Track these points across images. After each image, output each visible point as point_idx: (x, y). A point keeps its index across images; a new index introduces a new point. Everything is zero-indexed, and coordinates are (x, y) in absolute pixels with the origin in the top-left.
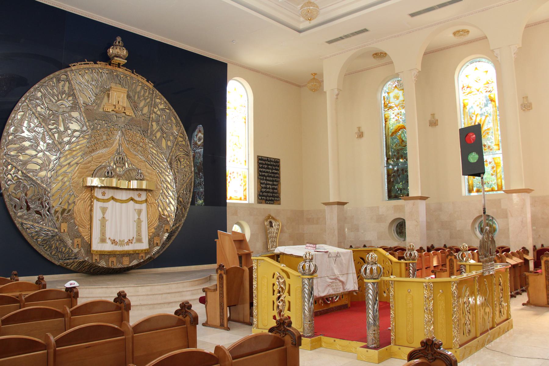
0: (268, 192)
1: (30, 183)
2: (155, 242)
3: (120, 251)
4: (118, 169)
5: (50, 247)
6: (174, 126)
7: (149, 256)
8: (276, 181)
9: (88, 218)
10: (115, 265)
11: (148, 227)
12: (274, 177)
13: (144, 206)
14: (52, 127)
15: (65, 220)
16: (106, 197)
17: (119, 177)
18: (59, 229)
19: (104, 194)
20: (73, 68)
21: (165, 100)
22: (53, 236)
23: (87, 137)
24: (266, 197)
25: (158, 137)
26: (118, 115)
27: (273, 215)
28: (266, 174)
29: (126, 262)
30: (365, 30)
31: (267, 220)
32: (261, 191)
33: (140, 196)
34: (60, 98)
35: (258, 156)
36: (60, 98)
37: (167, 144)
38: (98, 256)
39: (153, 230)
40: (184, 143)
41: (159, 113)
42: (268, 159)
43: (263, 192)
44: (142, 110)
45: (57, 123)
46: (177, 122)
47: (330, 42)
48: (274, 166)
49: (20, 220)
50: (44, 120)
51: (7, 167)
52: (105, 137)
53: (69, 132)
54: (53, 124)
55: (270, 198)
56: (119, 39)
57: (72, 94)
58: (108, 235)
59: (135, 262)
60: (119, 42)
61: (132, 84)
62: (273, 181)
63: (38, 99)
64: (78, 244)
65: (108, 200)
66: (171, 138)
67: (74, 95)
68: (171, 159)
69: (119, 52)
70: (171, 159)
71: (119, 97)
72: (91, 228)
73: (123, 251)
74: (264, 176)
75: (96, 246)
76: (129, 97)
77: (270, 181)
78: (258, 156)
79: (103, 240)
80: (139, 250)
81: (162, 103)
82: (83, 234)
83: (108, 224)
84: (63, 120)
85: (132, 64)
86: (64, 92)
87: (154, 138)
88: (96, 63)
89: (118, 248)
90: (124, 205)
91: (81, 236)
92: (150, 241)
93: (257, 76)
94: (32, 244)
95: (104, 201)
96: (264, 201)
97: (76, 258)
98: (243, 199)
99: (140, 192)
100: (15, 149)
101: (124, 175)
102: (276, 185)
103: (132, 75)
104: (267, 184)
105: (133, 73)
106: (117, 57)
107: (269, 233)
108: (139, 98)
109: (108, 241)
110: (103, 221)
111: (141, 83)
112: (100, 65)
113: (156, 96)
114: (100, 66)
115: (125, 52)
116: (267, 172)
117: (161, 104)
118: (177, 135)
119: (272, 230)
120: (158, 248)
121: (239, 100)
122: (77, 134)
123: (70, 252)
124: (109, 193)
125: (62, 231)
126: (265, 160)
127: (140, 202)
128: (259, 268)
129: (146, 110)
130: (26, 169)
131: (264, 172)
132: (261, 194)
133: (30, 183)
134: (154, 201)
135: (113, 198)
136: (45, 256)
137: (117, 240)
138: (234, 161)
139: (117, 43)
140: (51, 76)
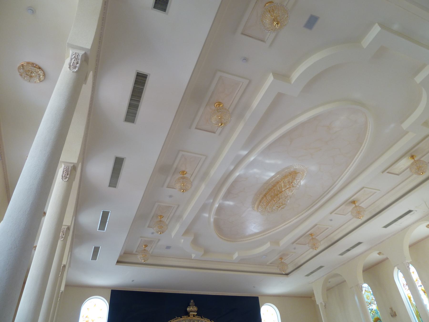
30: (321, 267)
47: (308, 275)
56: (192, 301)
69: (192, 309)
85: (200, 314)
88: (181, 318)
105: (202, 318)
106: (191, 312)
112: (185, 318)
115: (195, 309)
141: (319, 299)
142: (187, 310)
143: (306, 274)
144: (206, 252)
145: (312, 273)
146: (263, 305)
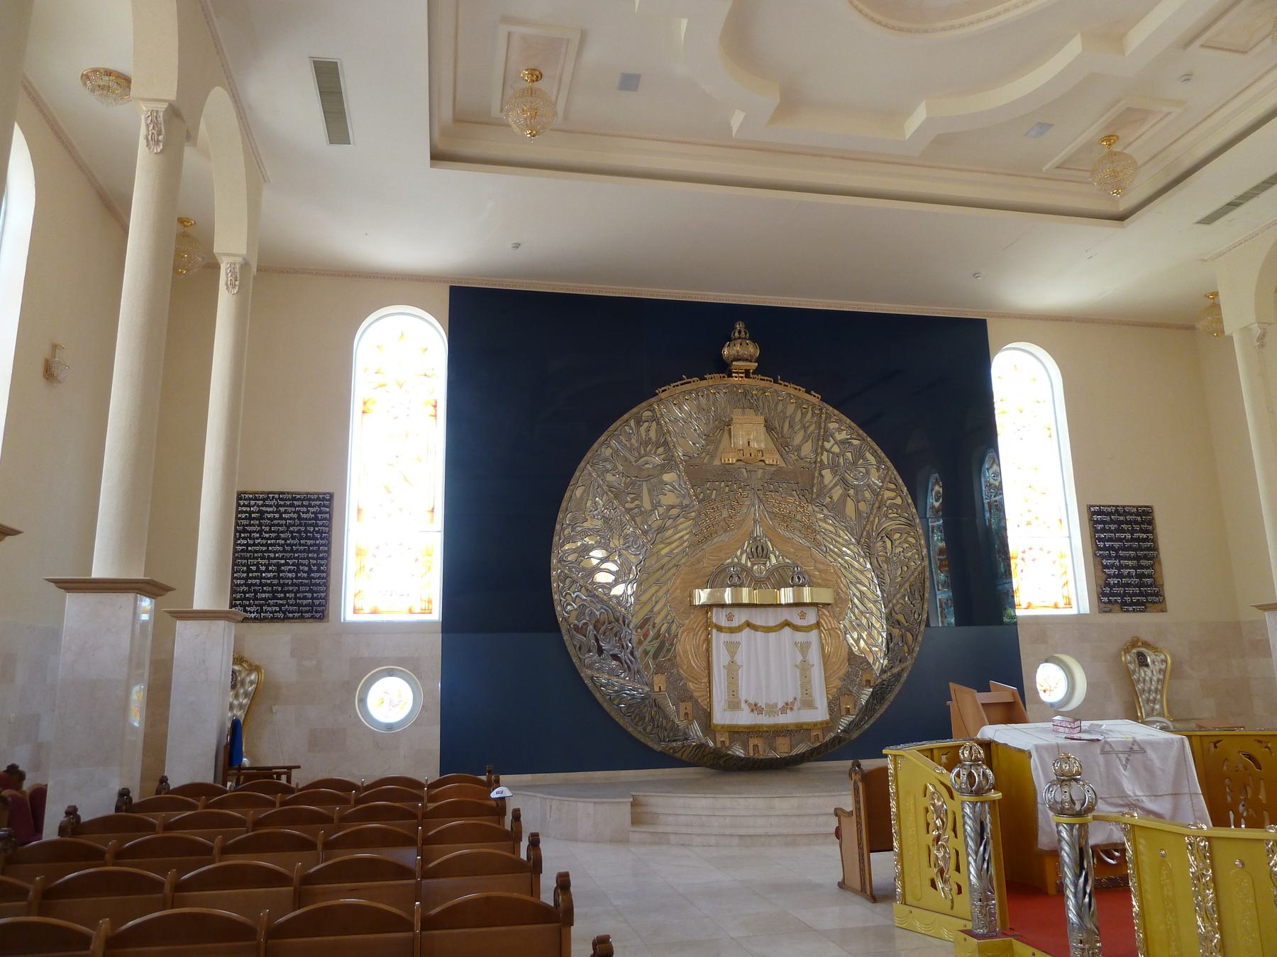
0: (1128, 585)
2: (843, 706)
3: (768, 726)
6: (873, 471)
8: (1145, 557)
9: (704, 664)
11: (826, 678)
12: (1140, 549)
13: (814, 633)
15: (659, 669)
16: (736, 623)
17: (757, 583)
18: (651, 686)
19: (730, 618)
20: (663, 395)
21: (848, 421)
22: (643, 699)
25: (836, 498)
28: (1117, 545)
29: (783, 749)
31: (1127, 651)
32: (1107, 585)
33: (803, 616)
37: (858, 511)
39: (838, 683)
40: (899, 501)
41: (836, 449)
42: (1118, 511)
43: (1111, 587)
44: (799, 449)
45: (638, 497)
46: (880, 461)
47: (1209, 220)
49: (589, 672)
50: (617, 494)
51: (564, 582)
52: (725, 514)
53: (661, 510)
54: (633, 500)
56: (739, 326)
57: (664, 444)
58: (743, 695)
59: (801, 749)
60: (740, 332)
61: (777, 404)
62: (1138, 558)
63: (605, 460)
66: (867, 495)
67: (666, 443)
68: (869, 536)
69: (741, 350)
70: (869, 536)
71: (749, 435)
72: (710, 682)
73: (774, 726)
75: (721, 717)
76: (769, 428)
77: (1129, 558)
79: (734, 705)
80: (808, 724)
81: (841, 430)
82: (696, 694)
83: (742, 675)
85: (768, 367)
87: (828, 500)
91: (691, 697)
92: (833, 705)
93: (1057, 330)
94: (613, 714)
95: (732, 630)
96: (1117, 607)
98: (1061, 605)
99: (805, 609)
100: (574, 551)
102: (1148, 568)
104: (1121, 567)
105: (776, 382)
108: (791, 426)
109: (743, 705)
111: (791, 399)
112: (713, 380)
113: (829, 417)
115: (752, 349)
116: (1119, 540)
117: (840, 430)
118: (881, 488)
119: (1146, 673)
121: (1026, 393)
122: (674, 512)
123: (675, 728)
124: (740, 617)
125: (657, 689)
127: (808, 629)
129: (807, 449)
130: (593, 583)
131: (1110, 540)
132: (1107, 590)
134: (834, 623)
135: (748, 624)
136: (635, 734)
137: (762, 704)
138: (1029, 523)
140: (626, 416)
141: (1238, 316)
143: (1198, 218)
144: (791, 102)
145: (1233, 205)
146: (998, 350)
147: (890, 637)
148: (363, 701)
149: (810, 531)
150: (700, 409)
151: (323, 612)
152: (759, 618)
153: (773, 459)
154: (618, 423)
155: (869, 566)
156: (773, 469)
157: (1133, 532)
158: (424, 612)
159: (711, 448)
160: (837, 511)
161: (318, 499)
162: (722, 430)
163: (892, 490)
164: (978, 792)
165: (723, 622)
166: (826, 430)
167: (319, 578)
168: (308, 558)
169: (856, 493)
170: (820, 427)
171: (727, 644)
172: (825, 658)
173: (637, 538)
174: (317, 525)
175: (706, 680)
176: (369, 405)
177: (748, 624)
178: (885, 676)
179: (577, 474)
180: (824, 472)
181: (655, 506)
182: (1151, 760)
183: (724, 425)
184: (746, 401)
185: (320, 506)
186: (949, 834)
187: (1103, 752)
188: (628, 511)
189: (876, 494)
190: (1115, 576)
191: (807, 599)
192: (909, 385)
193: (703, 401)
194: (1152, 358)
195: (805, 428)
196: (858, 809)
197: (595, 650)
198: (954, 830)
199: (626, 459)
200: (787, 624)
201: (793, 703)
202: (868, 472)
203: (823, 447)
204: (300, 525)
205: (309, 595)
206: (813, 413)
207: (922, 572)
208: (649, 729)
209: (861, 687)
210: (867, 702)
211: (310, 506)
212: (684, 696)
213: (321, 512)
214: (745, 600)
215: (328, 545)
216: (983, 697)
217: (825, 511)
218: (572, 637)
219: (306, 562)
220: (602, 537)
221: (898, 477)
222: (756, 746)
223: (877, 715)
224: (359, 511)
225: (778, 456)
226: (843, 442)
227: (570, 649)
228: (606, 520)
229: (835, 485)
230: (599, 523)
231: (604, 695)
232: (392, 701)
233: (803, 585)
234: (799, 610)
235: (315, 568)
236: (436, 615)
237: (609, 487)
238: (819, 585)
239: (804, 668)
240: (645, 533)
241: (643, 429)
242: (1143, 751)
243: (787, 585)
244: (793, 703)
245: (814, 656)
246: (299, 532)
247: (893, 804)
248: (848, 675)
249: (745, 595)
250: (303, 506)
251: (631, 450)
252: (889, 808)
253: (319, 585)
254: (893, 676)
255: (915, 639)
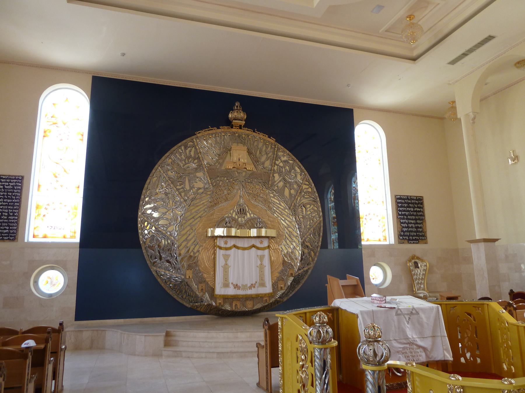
0: (412, 231)
1: (161, 236)
2: (279, 286)
3: (243, 295)
4: (240, 219)
5: (181, 291)
7: (273, 299)
8: (419, 219)
9: (212, 265)
10: (238, 307)
11: (272, 272)
12: (417, 215)
13: (267, 251)
14: (180, 187)
15: (190, 267)
16: (228, 245)
17: (240, 226)
18: (185, 276)
19: (226, 243)
20: (199, 135)
21: (288, 152)
22: (181, 282)
23: (209, 193)
24: (409, 236)
26: (239, 171)
27: (418, 254)
28: (407, 213)
29: (249, 306)
31: (410, 261)
32: (402, 231)
33: (261, 242)
34: (187, 162)
35: (396, 196)
36: (187, 162)
38: (222, 300)
39: (277, 275)
40: (310, 190)
41: (281, 164)
42: (409, 198)
43: (404, 232)
45: (183, 183)
46: (302, 171)
47: (453, 62)
48: (416, 203)
49: (155, 268)
53: (194, 190)
55: (414, 238)
56: (237, 104)
57: (198, 158)
58: (231, 280)
59: (258, 306)
60: (237, 107)
61: (254, 142)
62: (416, 219)
63: (168, 165)
64: (202, 289)
65: (230, 248)
66: (295, 186)
67: (198, 158)
68: (295, 205)
69: (237, 115)
70: (295, 205)
71: (239, 155)
72: (214, 274)
73: (246, 295)
74: (405, 215)
75: (219, 290)
76: (249, 153)
77: (412, 220)
78: (396, 196)
80: (262, 294)
81: (285, 156)
82: (207, 280)
83: (231, 270)
84: (189, 181)
86: (190, 157)
87: (276, 188)
88: (218, 128)
89: (240, 292)
90: (246, 252)
91: (205, 281)
92: (275, 286)
93: (384, 115)
94: (166, 289)
95: (226, 249)
96: (406, 241)
97: (202, 302)
98: (382, 240)
99: (262, 239)
100: (150, 208)
101: (245, 224)
102: (420, 224)
103: (254, 134)
104: (409, 223)
105: (254, 132)
106: (236, 120)
107: (414, 274)
108: (260, 153)
109: (231, 285)
110: (226, 268)
111: (262, 141)
112: (224, 129)
113: (278, 149)
114: (222, 130)
115: (242, 115)
117: (284, 156)
118: (301, 183)
119: (417, 271)
120: (283, 291)
121: (370, 142)
122: (201, 191)
123: (196, 296)
124: (231, 242)
125: (188, 277)
126: (404, 199)
127: (264, 249)
128: (284, 328)
129: (267, 164)
130: (159, 225)
131: (404, 211)
132: (402, 233)
133: (161, 236)
134: (276, 246)
135: (235, 246)
137: (240, 284)
138: (369, 203)
139: (236, 108)
140: (180, 144)
141: (464, 109)
142: (228, 117)
143: (449, 61)
145: (465, 55)
146: (357, 124)
147: (303, 254)
148: (36, 282)
149: (266, 202)
150: (216, 142)
151: (15, 236)
152: (240, 243)
153: (250, 167)
154: (175, 147)
155: (294, 219)
156: (251, 172)
157: (414, 208)
158: (72, 237)
159: (221, 161)
160: (280, 193)
161: (15, 179)
162: (227, 153)
163: (307, 185)
164: (323, 342)
165: (222, 245)
166: (277, 155)
167: (14, 219)
168: (8, 209)
169: (290, 186)
170: (274, 154)
171: (223, 255)
172: (272, 263)
173: (181, 203)
174: (14, 192)
175: (212, 273)
176: (47, 133)
177: (235, 246)
178: (300, 272)
179: (154, 171)
180: (275, 175)
181: (192, 188)
182: (422, 318)
183: (228, 150)
184: (240, 140)
185: (16, 182)
186: (309, 364)
187: (397, 314)
188: (178, 190)
189: (299, 186)
190: (406, 227)
191: (263, 234)
192: (317, 137)
193: (218, 139)
194: (425, 129)
195: (267, 154)
196: (266, 345)
197: (158, 258)
198: (311, 362)
199: (178, 165)
200: (254, 246)
201: (255, 284)
202: (296, 176)
203: (275, 163)
204: (4, 192)
205: (8, 228)
206: (271, 147)
207: (320, 223)
208: (184, 296)
209: (288, 276)
210: (291, 284)
211: (10, 182)
212: (201, 281)
213: (16, 186)
214: (233, 234)
215: (20, 202)
216: (342, 282)
217: (275, 193)
218: (147, 251)
219: (7, 211)
220: (164, 202)
221: (310, 179)
222: (236, 305)
223: (296, 290)
224: (39, 186)
225: (253, 166)
226: (285, 161)
227: (146, 257)
228: (166, 194)
229: (280, 181)
230: (164, 196)
231: (162, 280)
232: (52, 282)
233: (262, 228)
234: (260, 239)
235: (11, 214)
236: (77, 240)
237: (169, 178)
238: (270, 228)
239: (261, 267)
240: (185, 201)
241: (188, 151)
242: (417, 313)
243: (255, 228)
244: (255, 284)
245: (266, 262)
246: (3, 195)
247: (280, 345)
248: (282, 271)
249: (233, 232)
250: (6, 182)
251: (181, 161)
252: (278, 347)
253: (13, 223)
254: (304, 271)
255: (315, 254)
